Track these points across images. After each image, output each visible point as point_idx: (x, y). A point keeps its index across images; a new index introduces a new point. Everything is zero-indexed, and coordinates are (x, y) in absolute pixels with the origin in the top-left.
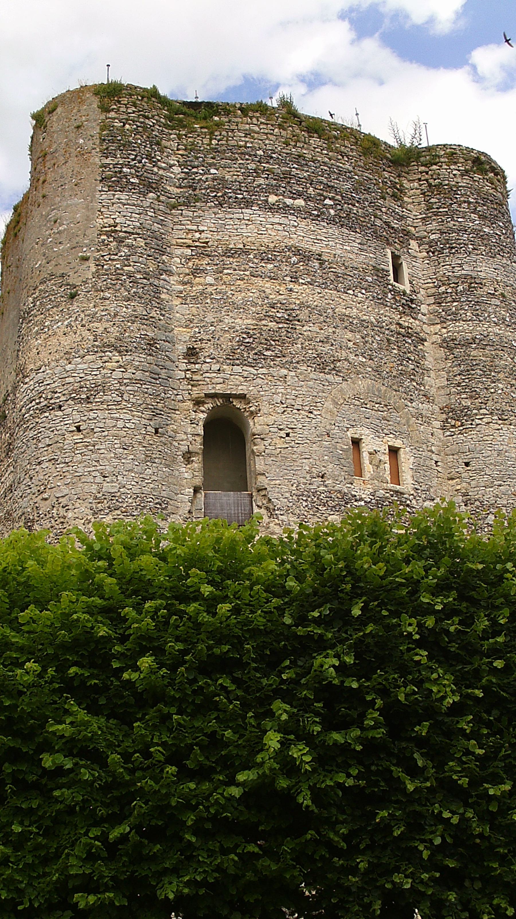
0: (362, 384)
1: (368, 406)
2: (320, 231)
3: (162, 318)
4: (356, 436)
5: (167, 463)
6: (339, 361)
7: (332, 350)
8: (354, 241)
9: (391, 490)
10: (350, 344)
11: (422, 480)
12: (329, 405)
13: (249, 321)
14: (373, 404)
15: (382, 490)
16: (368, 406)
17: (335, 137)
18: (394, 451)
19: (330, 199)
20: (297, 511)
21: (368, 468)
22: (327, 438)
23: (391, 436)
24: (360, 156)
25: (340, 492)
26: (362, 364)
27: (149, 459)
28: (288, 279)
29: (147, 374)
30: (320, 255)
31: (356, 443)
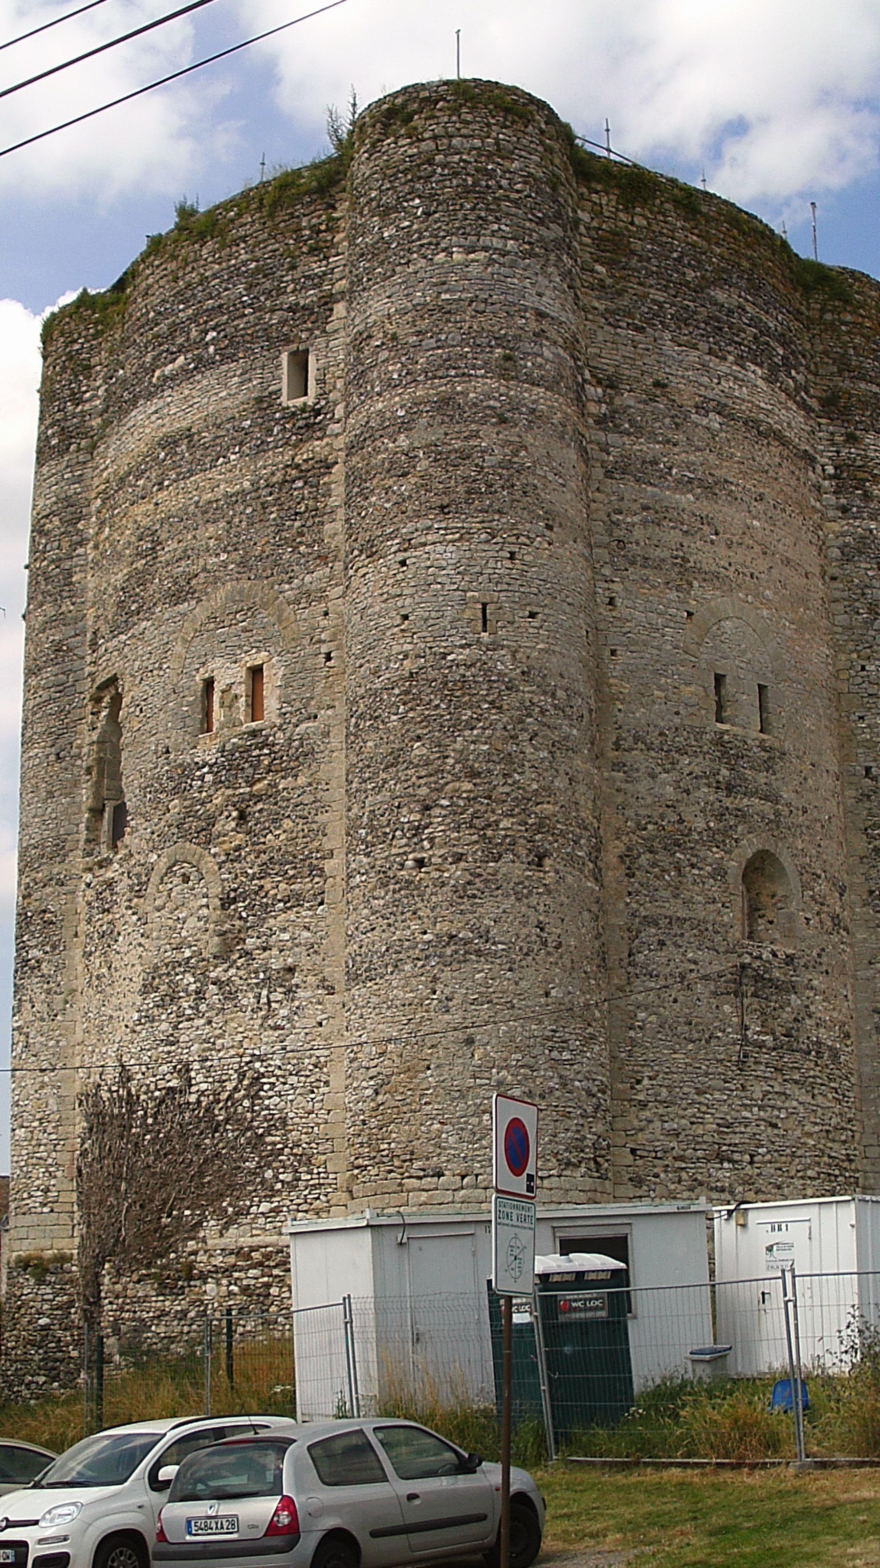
0: (220, 596)
1: (225, 624)
2: (194, 393)
3: (72, 608)
4: (207, 675)
5: (68, 791)
6: (196, 576)
7: (188, 566)
8: (234, 376)
9: (245, 733)
10: (212, 542)
11: (294, 697)
12: (179, 648)
13: (125, 571)
14: (231, 617)
15: (235, 737)
16: (225, 624)
17: (232, 221)
18: (256, 672)
19: (214, 329)
20: (143, 811)
21: (218, 714)
22: (173, 696)
23: (254, 651)
24: (264, 223)
25: (180, 765)
26: (224, 565)
27: (51, 794)
28: (155, 489)
29: (52, 690)
30: (189, 430)
31: (209, 684)
